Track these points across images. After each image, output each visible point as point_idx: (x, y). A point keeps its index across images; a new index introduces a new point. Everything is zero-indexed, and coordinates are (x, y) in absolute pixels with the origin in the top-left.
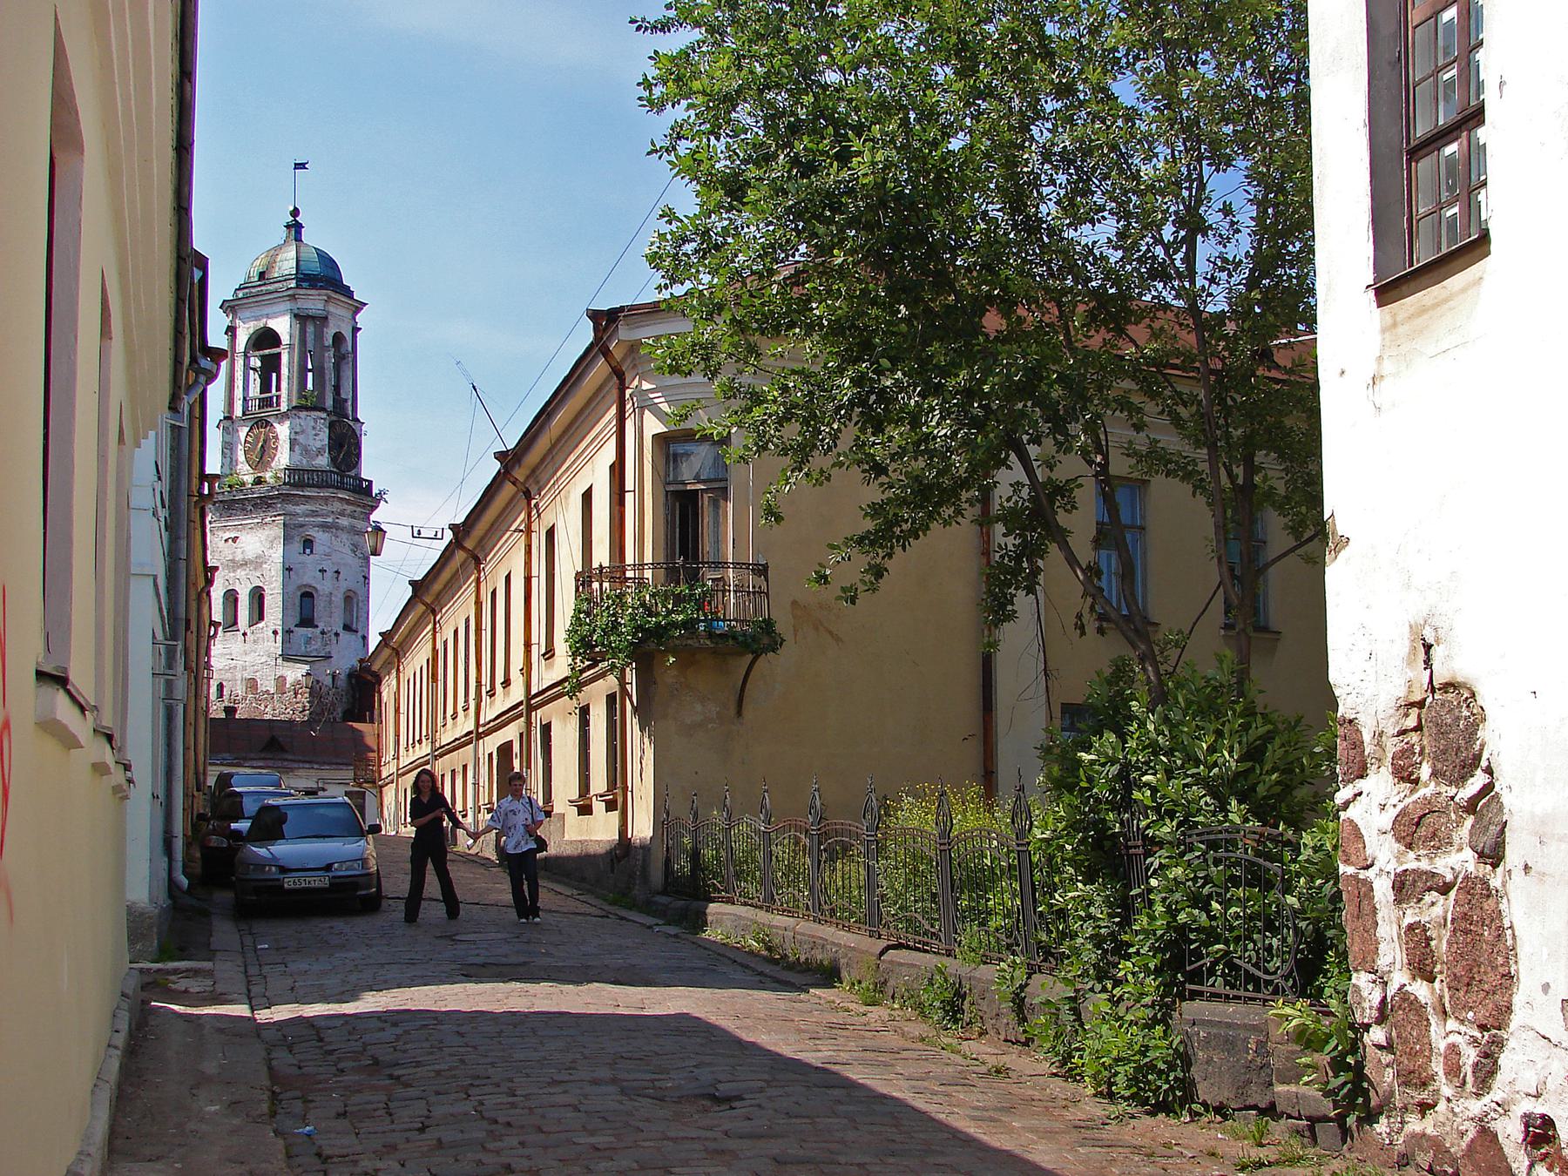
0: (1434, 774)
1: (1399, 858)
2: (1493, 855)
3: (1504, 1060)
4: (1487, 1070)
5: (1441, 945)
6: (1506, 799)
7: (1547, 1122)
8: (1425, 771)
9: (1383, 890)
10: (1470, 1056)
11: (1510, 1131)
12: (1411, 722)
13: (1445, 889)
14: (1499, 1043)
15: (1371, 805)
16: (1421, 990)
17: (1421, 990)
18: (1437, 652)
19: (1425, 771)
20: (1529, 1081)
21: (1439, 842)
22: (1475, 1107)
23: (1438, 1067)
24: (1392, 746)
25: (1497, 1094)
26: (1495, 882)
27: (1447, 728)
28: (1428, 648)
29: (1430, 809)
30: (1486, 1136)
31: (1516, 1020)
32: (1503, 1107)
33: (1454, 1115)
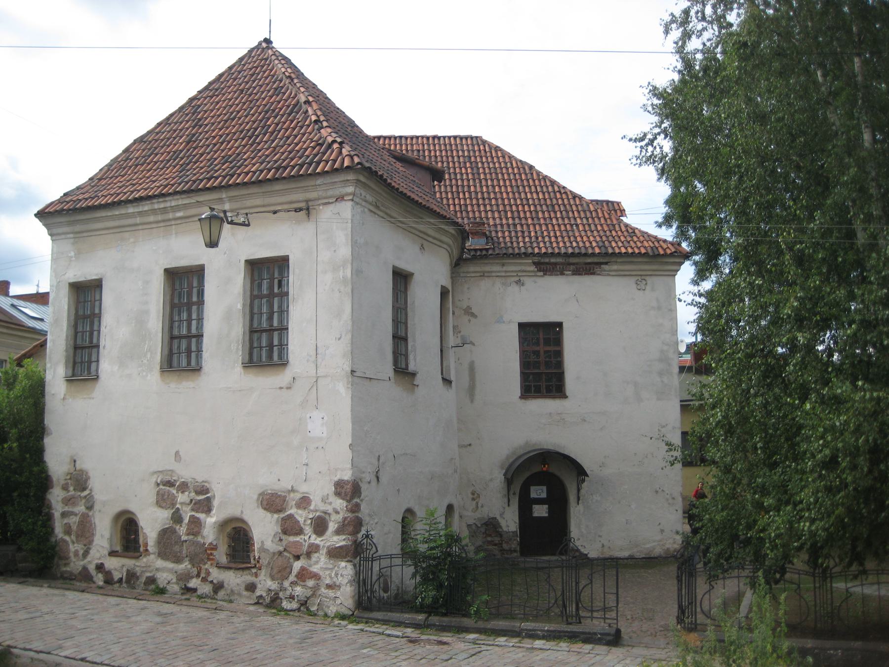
0: (74, 490)
1: (63, 508)
2: (90, 508)
3: (91, 552)
4: (86, 553)
5: (74, 527)
6: (96, 497)
7: (102, 564)
8: (71, 488)
9: (57, 515)
10: (81, 552)
11: (92, 568)
12: (68, 477)
13: (76, 515)
14: (90, 549)
15: (56, 496)
16: (67, 538)
17: (67, 538)
18: (78, 463)
19: (71, 488)
20: (98, 555)
21: (74, 504)
22: (82, 563)
23: (72, 555)
24: (63, 482)
25: (89, 559)
26: (91, 514)
27: (79, 481)
28: (75, 461)
29: (73, 497)
30: (85, 569)
31: (95, 543)
32: (90, 562)
33: (75, 565)
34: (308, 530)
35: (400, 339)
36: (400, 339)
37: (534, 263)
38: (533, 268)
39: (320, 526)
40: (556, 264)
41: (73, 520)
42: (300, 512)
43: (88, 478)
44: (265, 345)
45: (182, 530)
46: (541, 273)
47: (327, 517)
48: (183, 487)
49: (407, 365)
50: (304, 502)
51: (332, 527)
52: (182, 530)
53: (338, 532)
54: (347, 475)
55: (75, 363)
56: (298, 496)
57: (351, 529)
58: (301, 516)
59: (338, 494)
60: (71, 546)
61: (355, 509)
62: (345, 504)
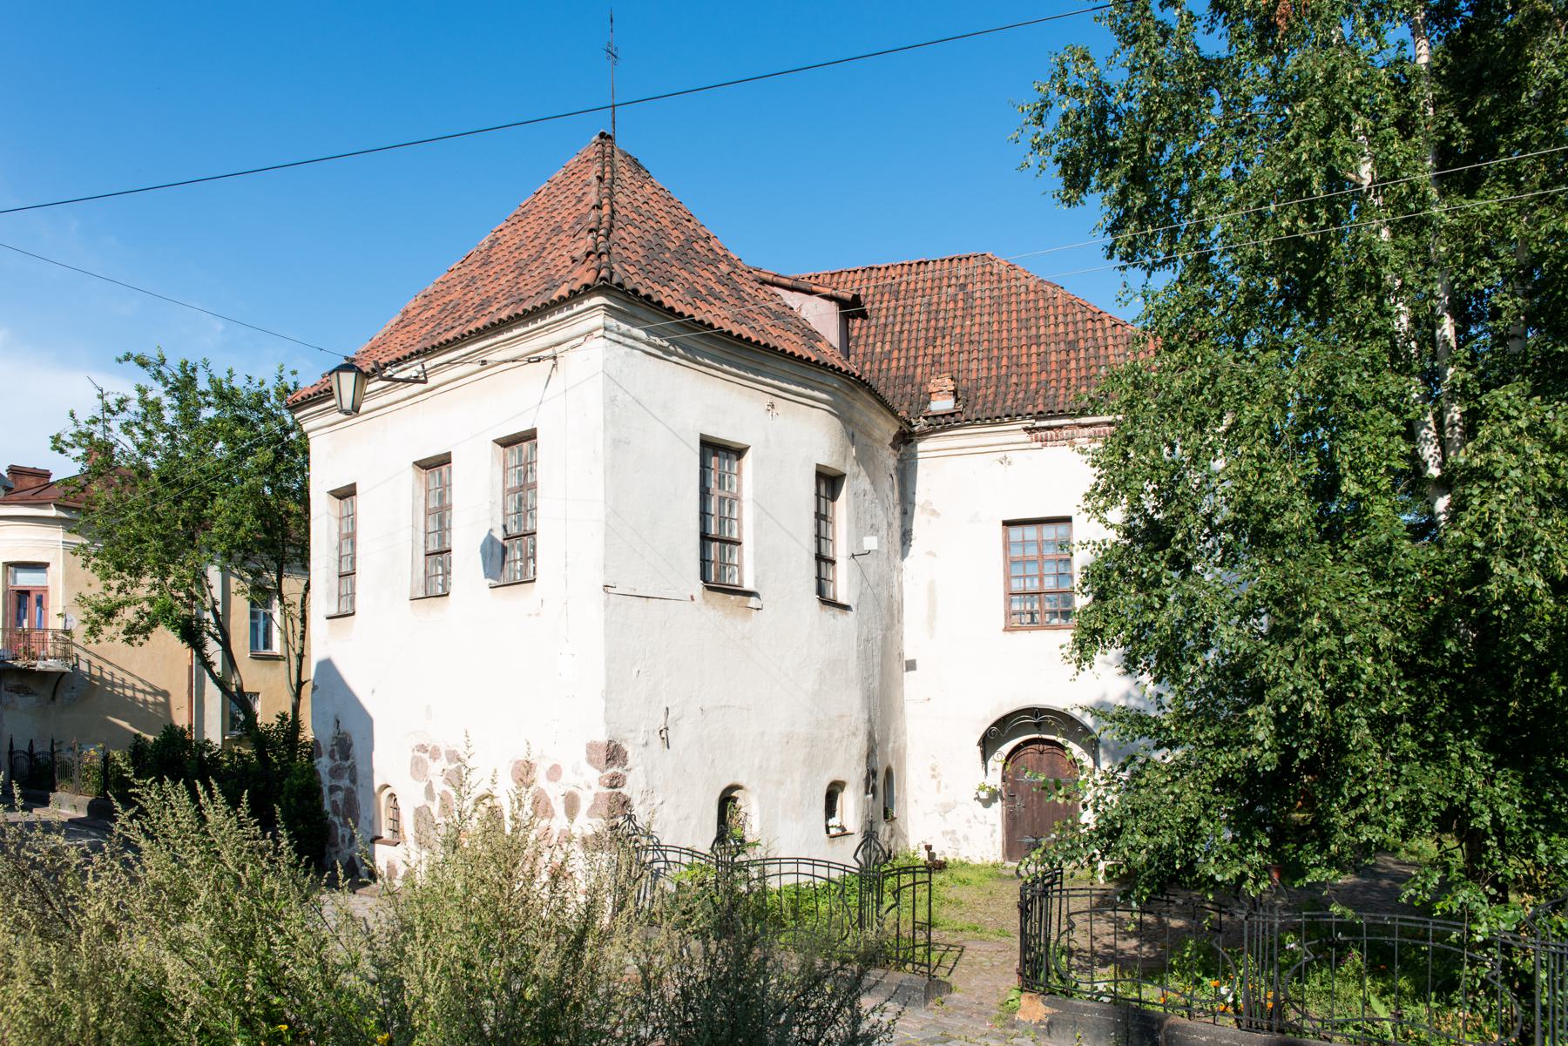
2: (353, 781)
9: (326, 791)
21: (341, 777)
34: (559, 807)
35: (714, 543)
36: (714, 543)
37: (1026, 429)
38: (1025, 436)
39: (571, 804)
40: (1060, 427)
41: (340, 796)
42: (551, 785)
43: (349, 745)
44: (509, 556)
45: (435, 808)
46: (1039, 444)
47: (579, 793)
48: (435, 754)
49: (741, 580)
50: (555, 772)
51: (585, 804)
52: (435, 808)
53: (592, 812)
54: (602, 738)
55: (340, 596)
56: (548, 765)
57: (604, 811)
58: (555, 793)
59: (590, 761)
60: (340, 831)
61: (615, 782)
62: (597, 774)
